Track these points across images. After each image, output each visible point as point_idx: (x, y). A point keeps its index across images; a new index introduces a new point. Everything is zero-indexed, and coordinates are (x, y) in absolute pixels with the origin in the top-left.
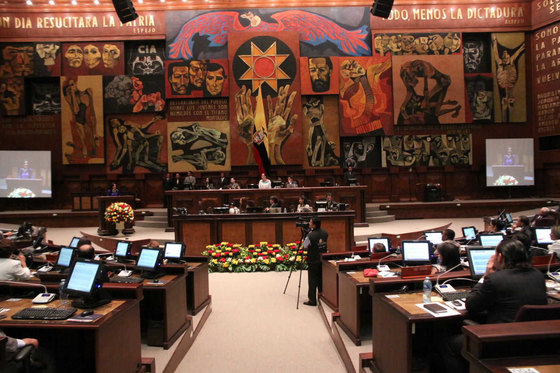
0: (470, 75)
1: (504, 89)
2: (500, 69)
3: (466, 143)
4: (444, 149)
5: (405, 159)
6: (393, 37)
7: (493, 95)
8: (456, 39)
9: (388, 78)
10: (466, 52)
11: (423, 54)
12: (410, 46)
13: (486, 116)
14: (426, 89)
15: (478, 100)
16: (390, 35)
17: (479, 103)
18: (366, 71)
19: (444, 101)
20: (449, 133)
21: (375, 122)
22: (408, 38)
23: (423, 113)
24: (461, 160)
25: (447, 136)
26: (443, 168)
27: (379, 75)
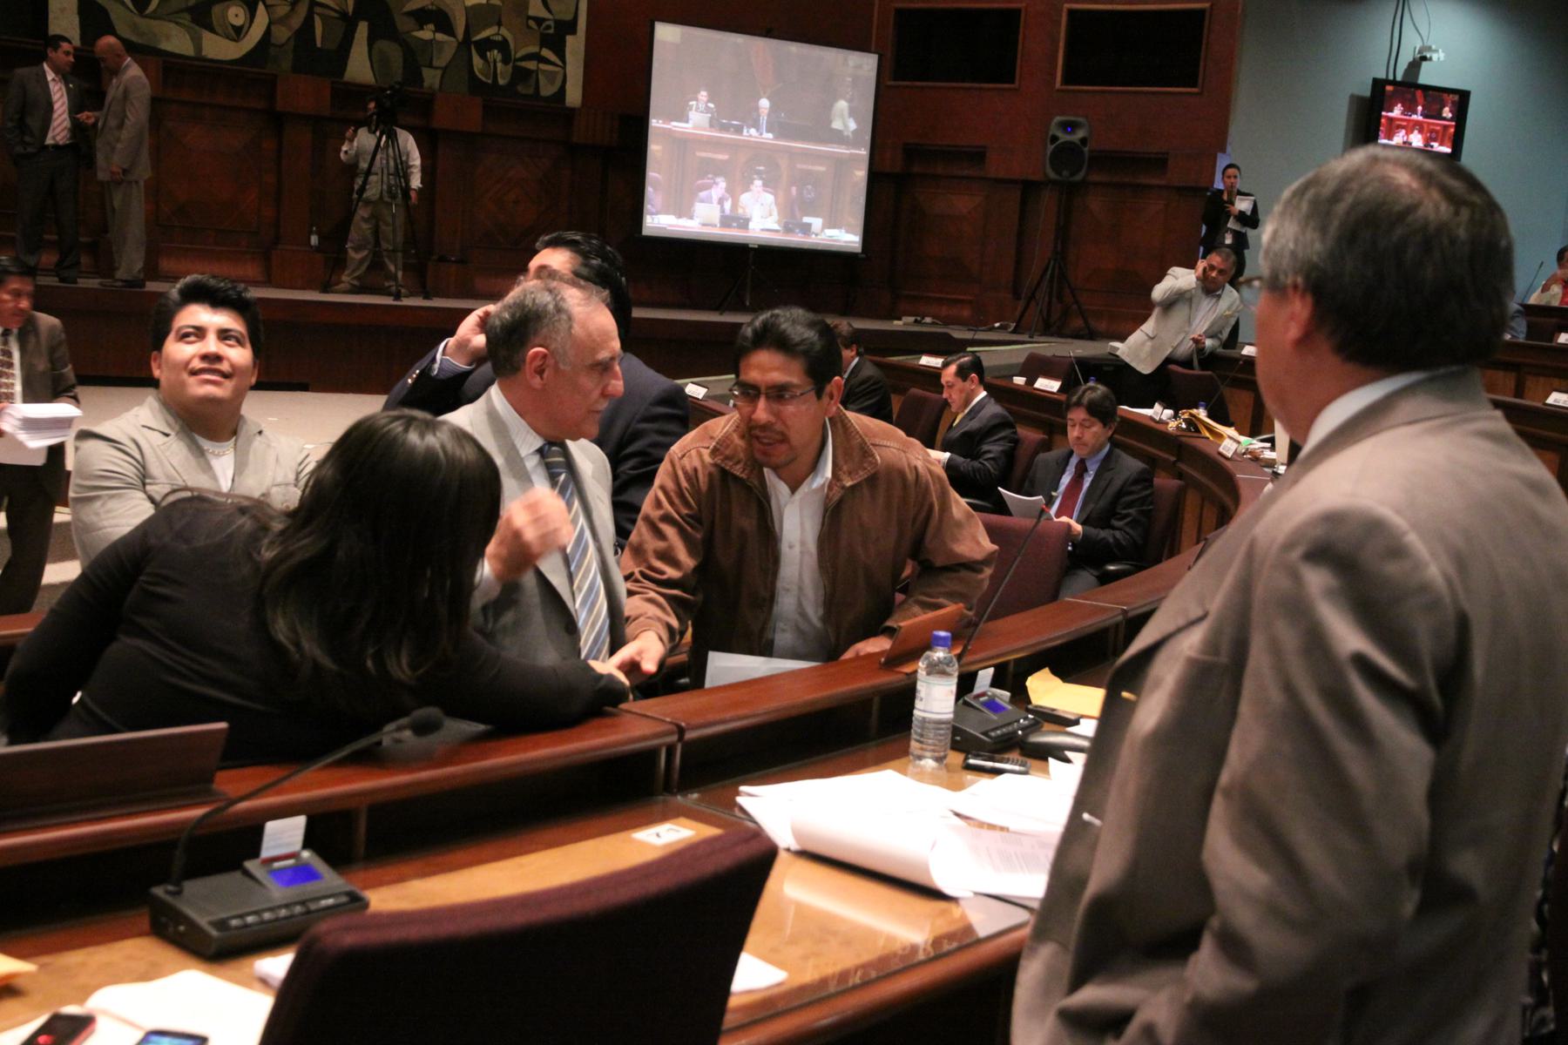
24: (529, 72)
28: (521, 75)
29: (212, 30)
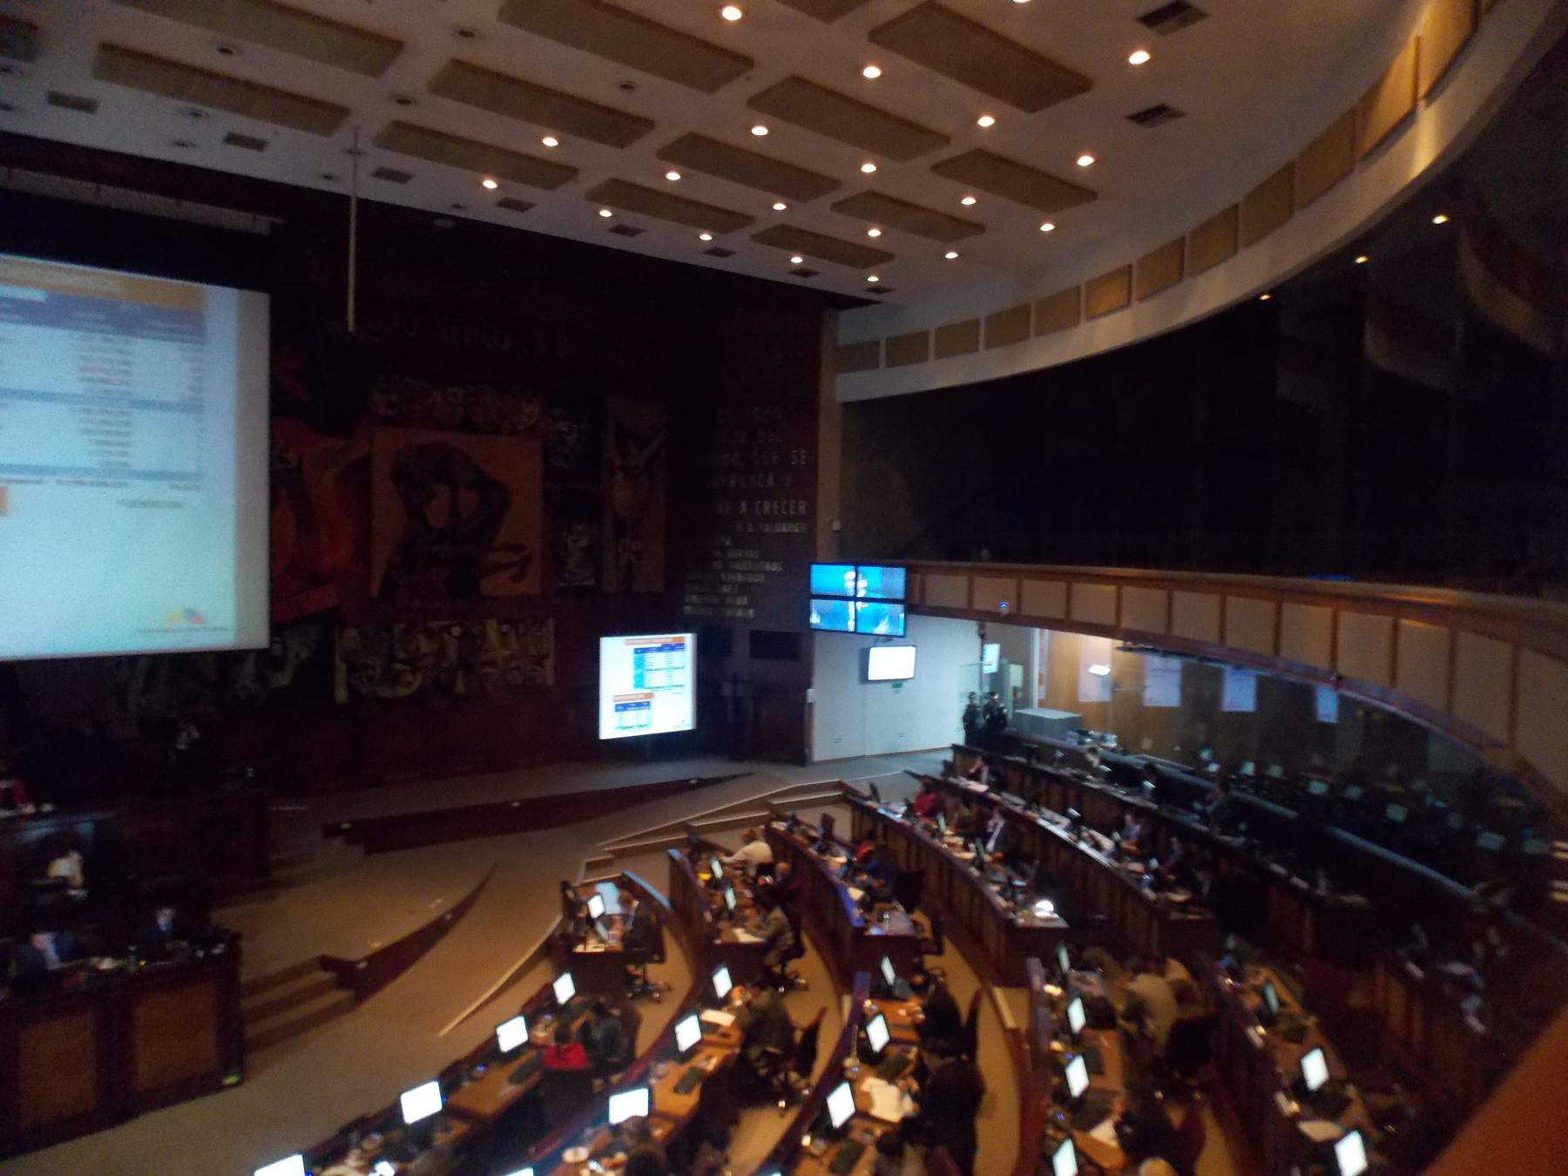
2: (619, 477)
5: (395, 679)
25: (500, 623)
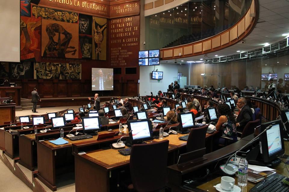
0: (81, 35)
1: (97, 44)
2: (96, 34)
3: (79, 68)
4: (68, 71)
5: (47, 75)
6: (43, 9)
7: (92, 46)
8: (76, 16)
9: (39, 31)
10: (81, 23)
11: (59, 20)
12: (52, 16)
13: (88, 56)
14: (59, 39)
15: (85, 47)
16: (42, 7)
17: (85, 49)
18: (27, 25)
19: (68, 46)
20: (70, 62)
21: (30, 54)
22: (52, 11)
23: (57, 52)
25: (69, 65)
26: (67, 80)
27: (34, 28)
28: (75, 77)
29: (47, 76)
